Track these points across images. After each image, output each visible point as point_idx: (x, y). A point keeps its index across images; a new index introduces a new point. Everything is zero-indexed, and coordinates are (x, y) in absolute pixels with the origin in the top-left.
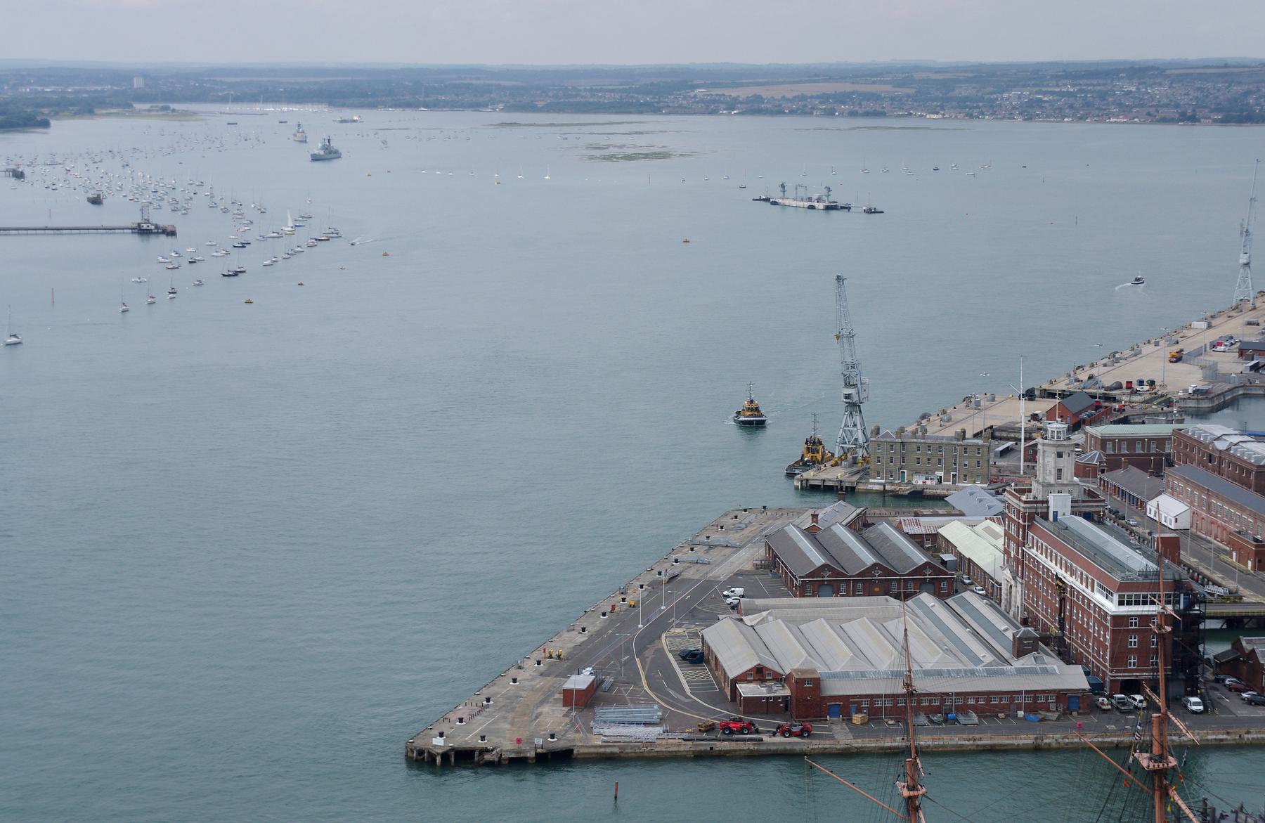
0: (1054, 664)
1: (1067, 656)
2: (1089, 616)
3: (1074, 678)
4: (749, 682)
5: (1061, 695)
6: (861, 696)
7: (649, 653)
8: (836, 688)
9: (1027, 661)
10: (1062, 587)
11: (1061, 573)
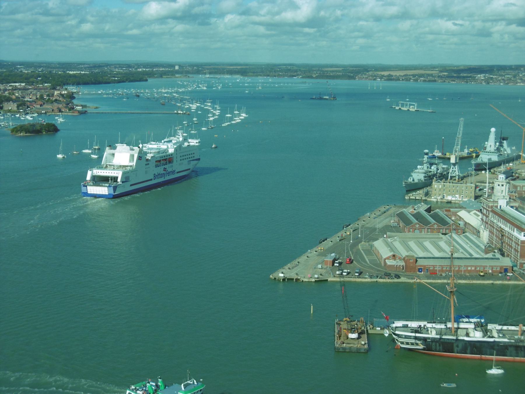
0: (498, 255)
1: (503, 255)
2: (512, 241)
3: (507, 262)
4: (391, 259)
5: (501, 267)
6: (430, 266)
7: (354, 250)
8: (420, 262)
9: (490, 255)
10: (501, 231)
11: (503, 226)
